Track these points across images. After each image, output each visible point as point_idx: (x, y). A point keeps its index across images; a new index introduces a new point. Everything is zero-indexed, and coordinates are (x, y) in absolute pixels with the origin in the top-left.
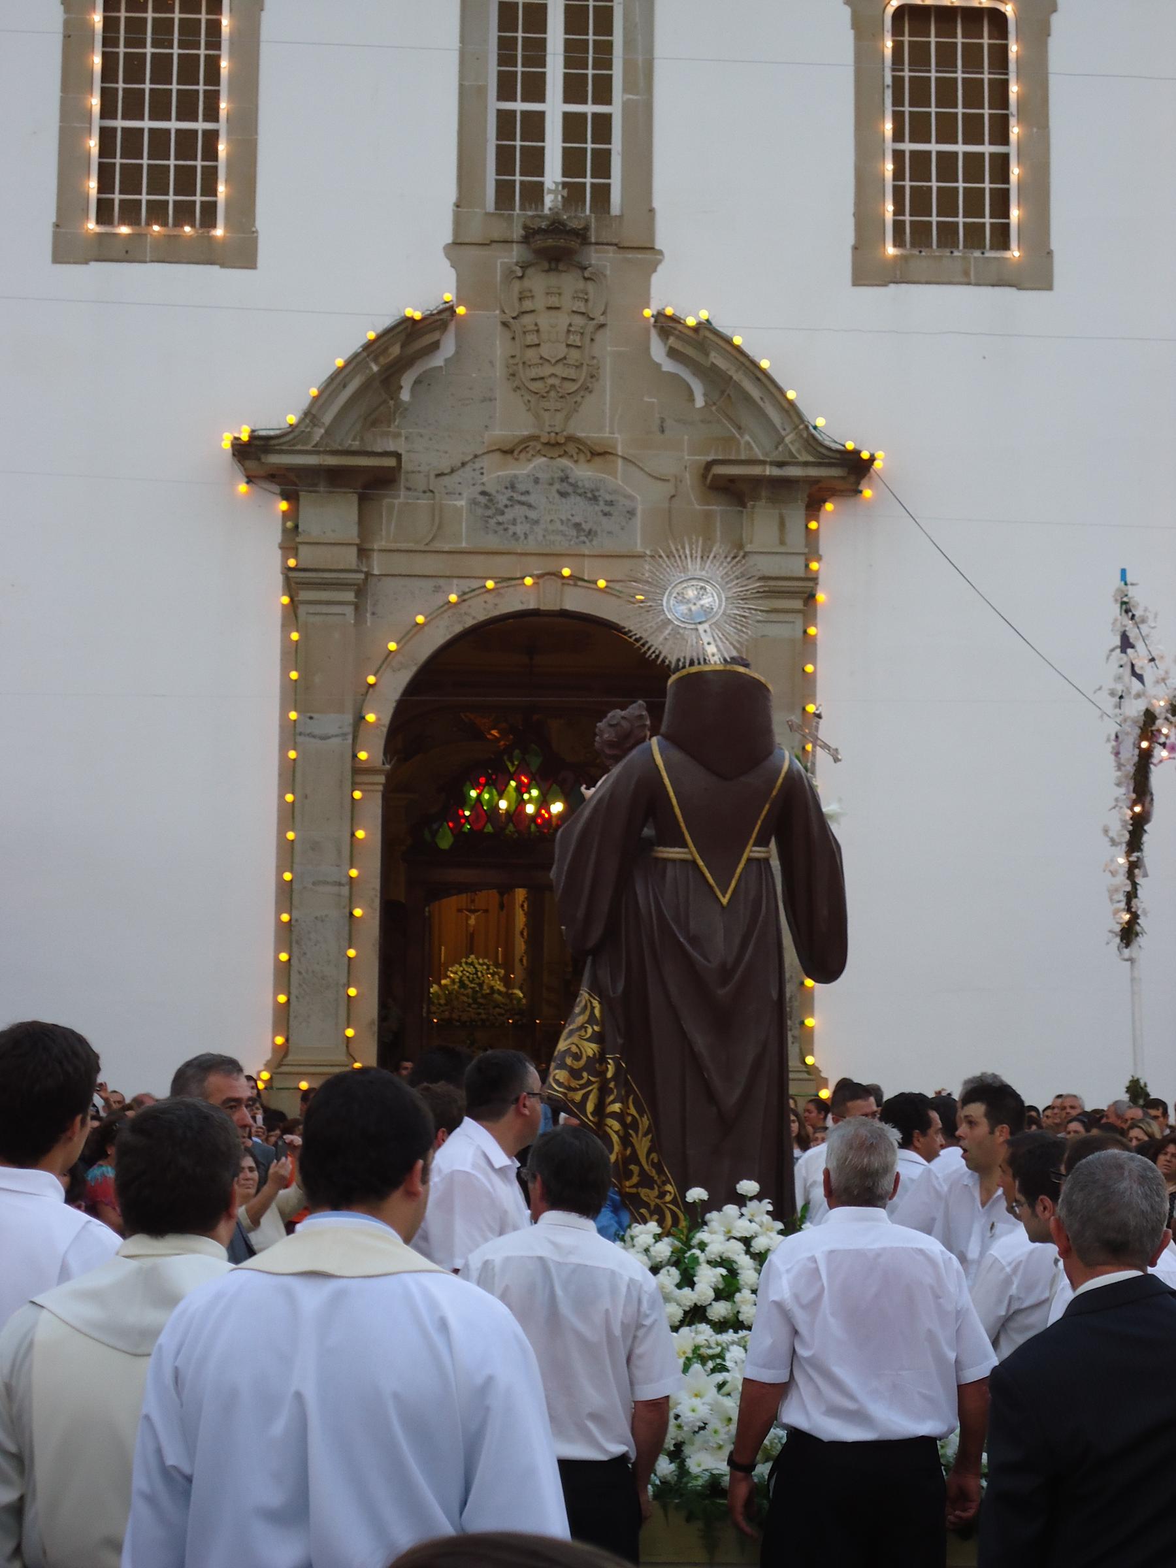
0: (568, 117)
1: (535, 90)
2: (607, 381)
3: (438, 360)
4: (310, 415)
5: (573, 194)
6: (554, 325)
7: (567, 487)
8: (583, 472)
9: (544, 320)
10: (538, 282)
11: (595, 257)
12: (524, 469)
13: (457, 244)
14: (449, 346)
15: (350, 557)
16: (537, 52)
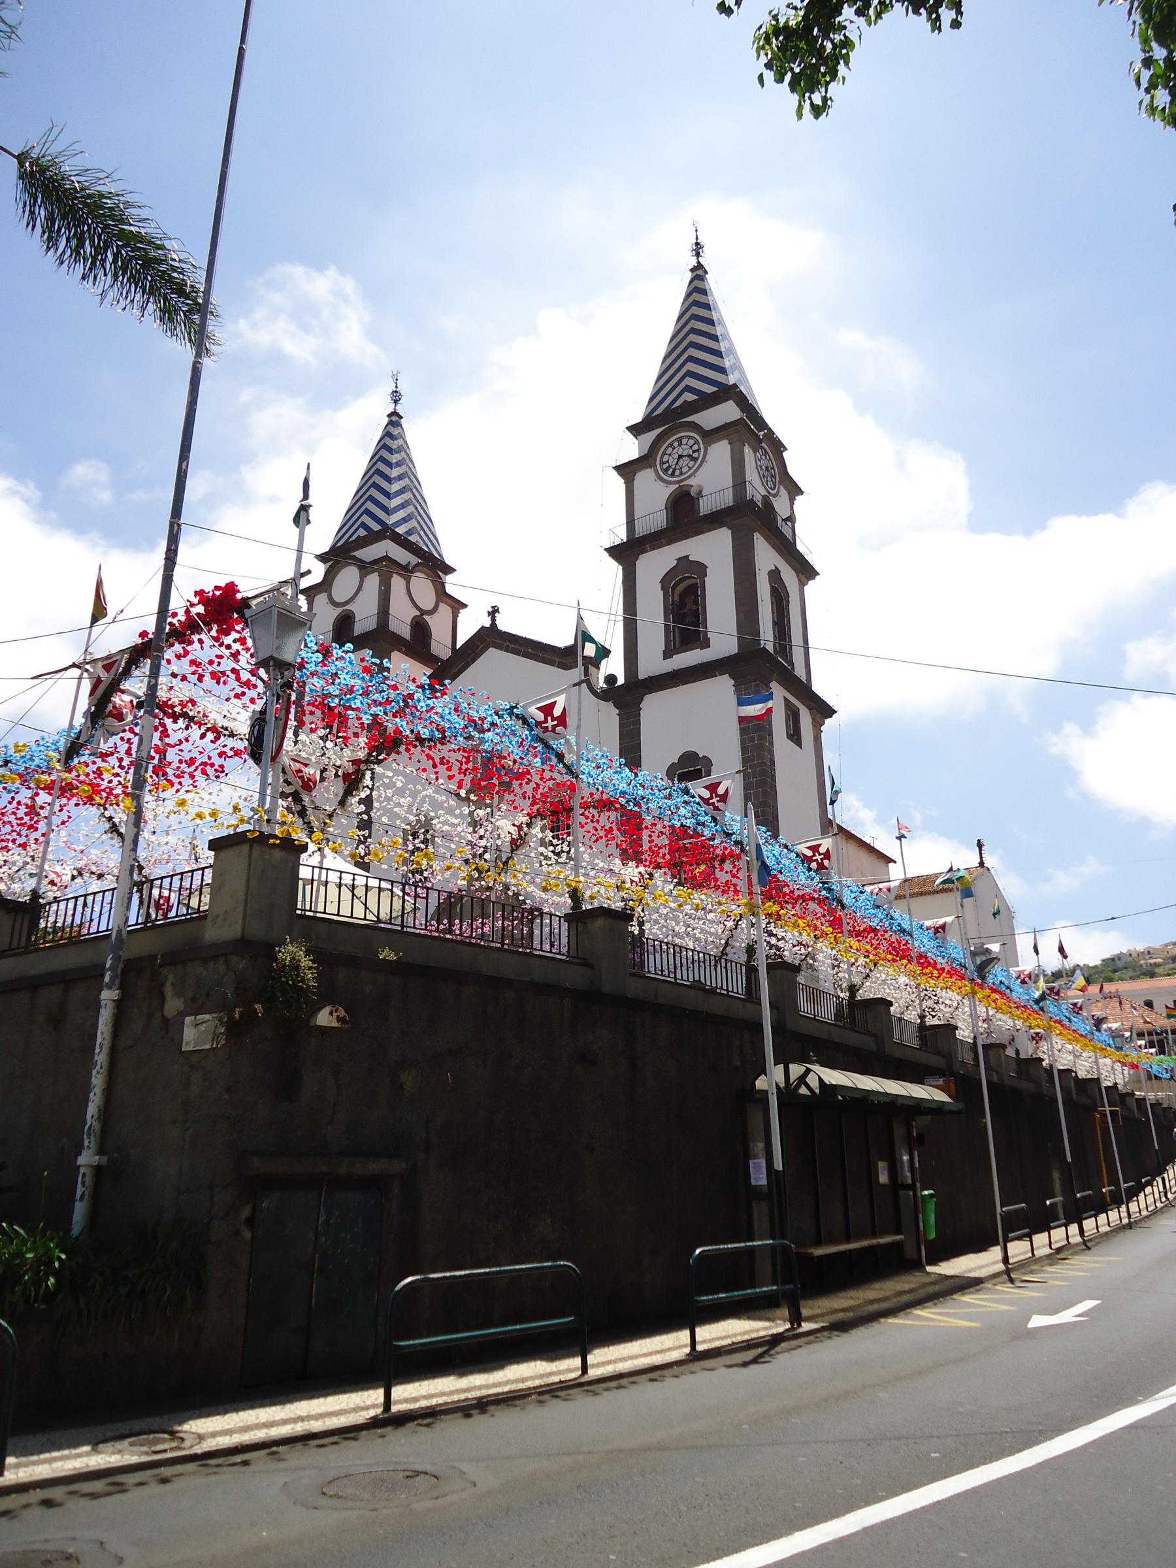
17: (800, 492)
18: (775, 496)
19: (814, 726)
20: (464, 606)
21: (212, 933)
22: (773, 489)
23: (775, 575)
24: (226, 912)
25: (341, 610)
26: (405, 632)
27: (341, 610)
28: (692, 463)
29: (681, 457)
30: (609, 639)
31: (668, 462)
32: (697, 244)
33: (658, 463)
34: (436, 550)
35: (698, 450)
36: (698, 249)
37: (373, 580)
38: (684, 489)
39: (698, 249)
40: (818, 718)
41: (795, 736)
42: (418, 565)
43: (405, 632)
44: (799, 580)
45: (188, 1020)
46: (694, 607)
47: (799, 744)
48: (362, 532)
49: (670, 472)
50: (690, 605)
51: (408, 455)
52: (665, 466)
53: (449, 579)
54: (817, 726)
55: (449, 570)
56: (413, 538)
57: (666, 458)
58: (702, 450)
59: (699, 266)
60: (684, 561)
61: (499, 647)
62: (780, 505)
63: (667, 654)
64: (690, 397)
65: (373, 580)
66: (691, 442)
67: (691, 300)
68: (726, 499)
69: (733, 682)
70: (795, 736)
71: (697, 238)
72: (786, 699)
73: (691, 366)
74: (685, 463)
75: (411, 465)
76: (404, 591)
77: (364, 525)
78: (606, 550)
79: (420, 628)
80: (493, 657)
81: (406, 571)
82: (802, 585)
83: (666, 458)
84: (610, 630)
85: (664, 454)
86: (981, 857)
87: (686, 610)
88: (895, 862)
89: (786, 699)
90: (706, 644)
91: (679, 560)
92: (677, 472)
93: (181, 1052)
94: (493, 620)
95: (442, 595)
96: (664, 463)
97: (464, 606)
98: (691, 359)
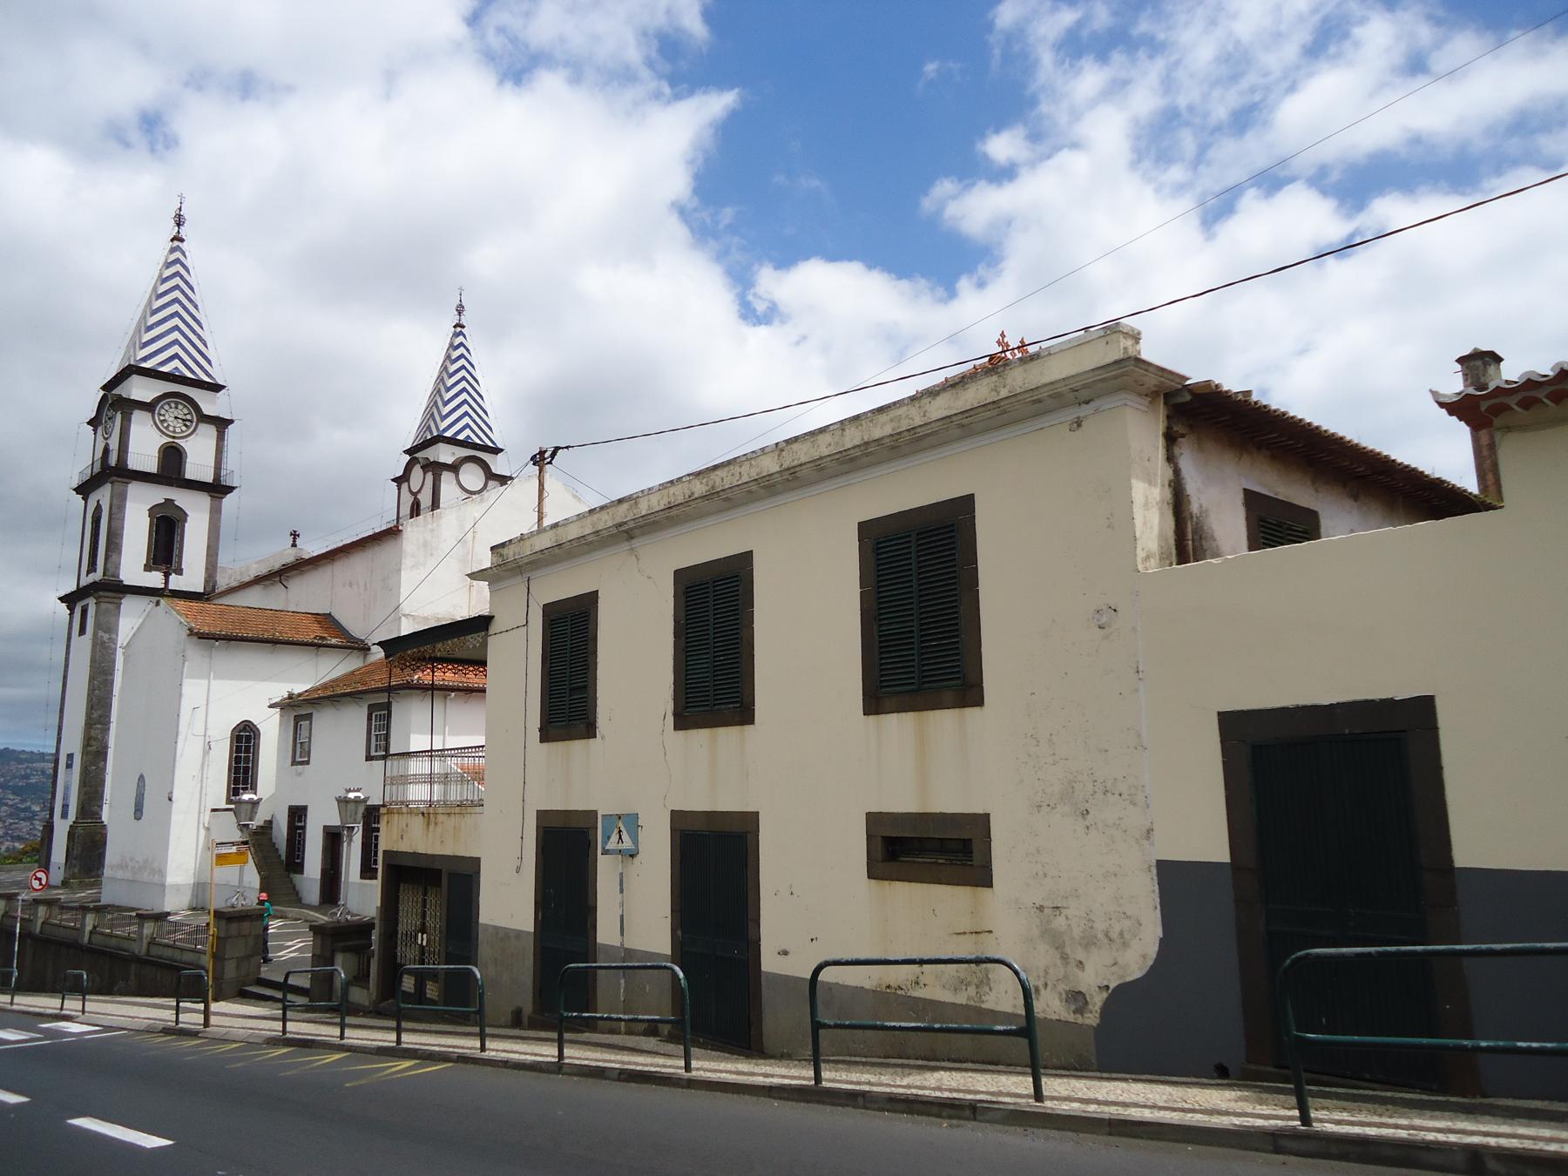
28: (184, 428)
33: (156, 412)
36: (179, 221)
39: (179, 221)
49: (165, 425)
52: (162, 418)
57: (163, 412)
58: (194, 424)
59: (177, 238)
60: (169, 502)
66: (186, 411)
74: (179, 425)
83: (163, 412)
85: (162, 407)
92: (171, 429)
96: (161, 415)
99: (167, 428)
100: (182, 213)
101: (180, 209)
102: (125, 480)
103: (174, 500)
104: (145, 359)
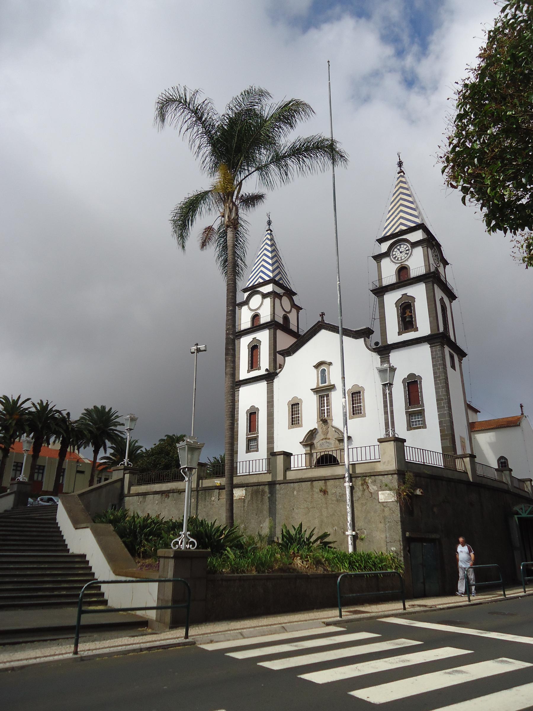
0: (327, 409)
1: (324, 407)
2: (329, 431)
3: (316, 433)
4: (304, 440)
5: (327, 415)
6: (324, 428)
7: (327, 442)
8: (328, 441)
9: (324, 428)
10: (323, 424)
11: (328, 421)
12: (324, 441)
13: (317, 422)
14: (317, 431)
15: (309, 452)
16: (324, 404)
17: (448, 264)
18: (439, 267)
19: (459, 361)
20: (301, 309)
21: (380, 468)
22: (438, 264)
23: (442, 300)
24: (388, 461)
25: (254, 312)
26: (281, 321)
27: (254, 312)
28: (406, 255)
29: (401, 252)
30: (372, 327)
31: (395, 254)
32: (400, 162)
33: (391, 255)
34: (289, 286)
35: (408, 250)
37: (268, 301)
38: (403, 266)
39: (400, 164)
40: (461, 358)
41: (453, 367)
42: (284, 293)
43: (281, 321)
44: (450, 301)
45: (380, 493)
46: (410, 314)
47: (455, 370)
48: (261, 281)
50: (408, 313)
51: (276, 247)
52: (394, 256)
53: (294, 298)
54: (460, 360)
55: (295, 294)
56: (281, 282)
57: (394, 253)
58: (410, 250)
61: (326, 329)
62: (441, 270)
63: (400, 333)
64: (404, 228)
65: (268, 301)
66: (405, 246)
67: (399, 186)
68: (422, 271)
69: (429, 346)
70: (453, 367)
71: (400, 159)
72: (449, 351)
73: (401, 214)
74: (403, 255)
75: (277, 252)
76: (280, 304)
77: (261, 277)
78: (371, 291)
79: (286, 318)
80: (323, 333)
81: (279, 296)
82: (451, 302)
84: (373, 322)
85: (393, 251)
86: (522, 411)
87: (406, 315)
88: (480, 412)
89: (449, 351)
90: (416, 330)
91: (403, 295)
92: (400, 259)
93: (379, 502)
94: (323, 318)
95: (294, 305)
96: (394, 255)
97: (301, 309)
98: (401, 211)
99: (398, 259)
100: (401, 160)
101: (400, 159)
102: (381, 294)
103: (406, 294)
104: (386, 233)
